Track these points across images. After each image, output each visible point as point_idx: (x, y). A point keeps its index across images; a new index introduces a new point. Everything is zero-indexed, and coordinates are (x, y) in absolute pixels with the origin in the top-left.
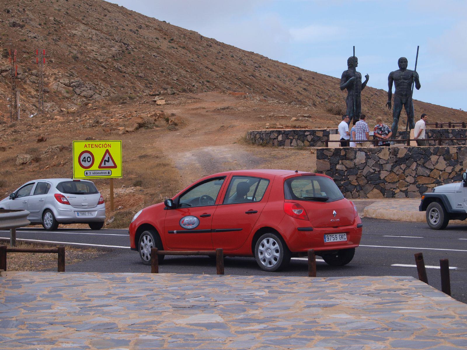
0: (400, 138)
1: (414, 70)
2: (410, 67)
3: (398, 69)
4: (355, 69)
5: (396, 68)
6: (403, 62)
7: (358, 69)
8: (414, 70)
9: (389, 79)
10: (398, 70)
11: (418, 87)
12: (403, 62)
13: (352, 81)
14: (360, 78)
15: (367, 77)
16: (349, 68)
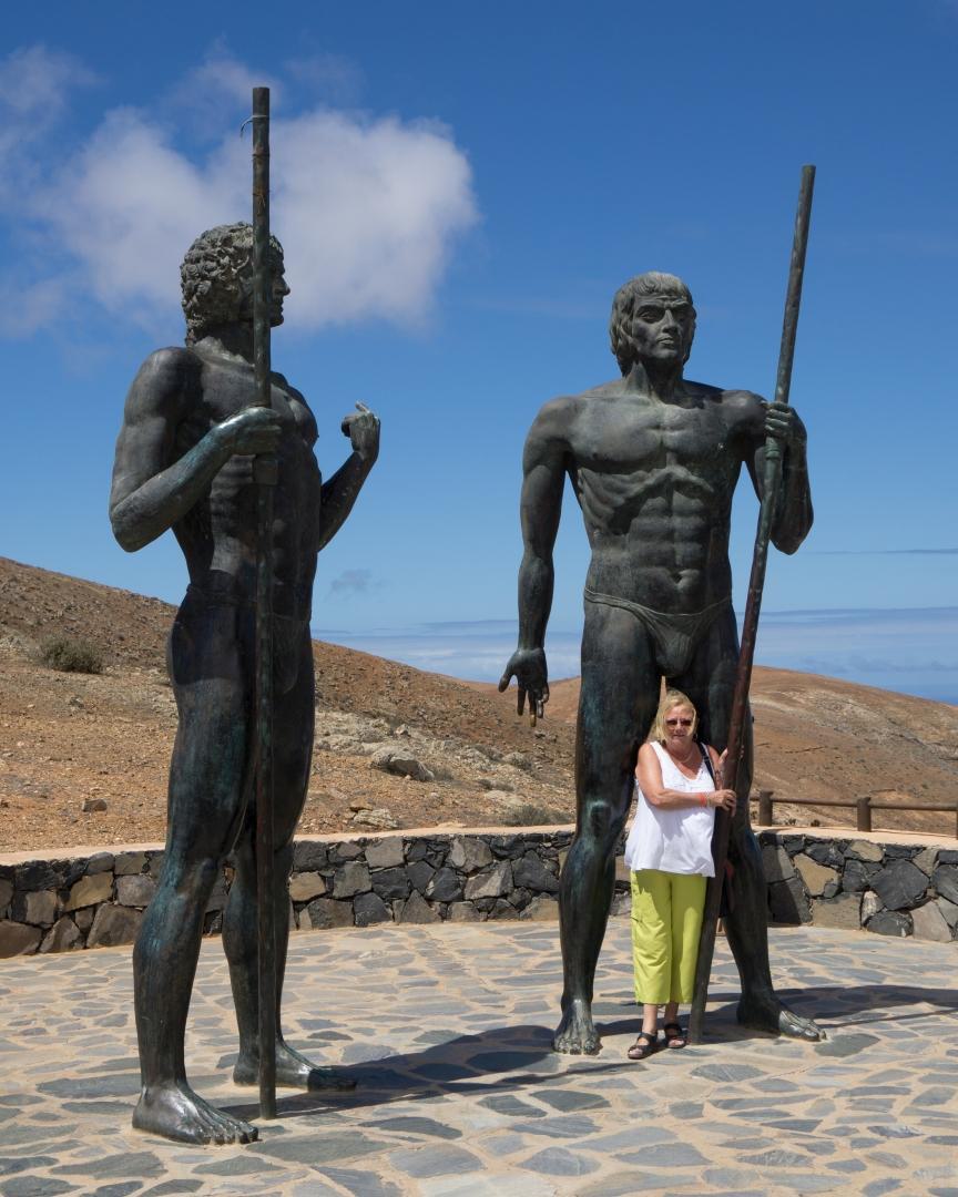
0: (492, 886)
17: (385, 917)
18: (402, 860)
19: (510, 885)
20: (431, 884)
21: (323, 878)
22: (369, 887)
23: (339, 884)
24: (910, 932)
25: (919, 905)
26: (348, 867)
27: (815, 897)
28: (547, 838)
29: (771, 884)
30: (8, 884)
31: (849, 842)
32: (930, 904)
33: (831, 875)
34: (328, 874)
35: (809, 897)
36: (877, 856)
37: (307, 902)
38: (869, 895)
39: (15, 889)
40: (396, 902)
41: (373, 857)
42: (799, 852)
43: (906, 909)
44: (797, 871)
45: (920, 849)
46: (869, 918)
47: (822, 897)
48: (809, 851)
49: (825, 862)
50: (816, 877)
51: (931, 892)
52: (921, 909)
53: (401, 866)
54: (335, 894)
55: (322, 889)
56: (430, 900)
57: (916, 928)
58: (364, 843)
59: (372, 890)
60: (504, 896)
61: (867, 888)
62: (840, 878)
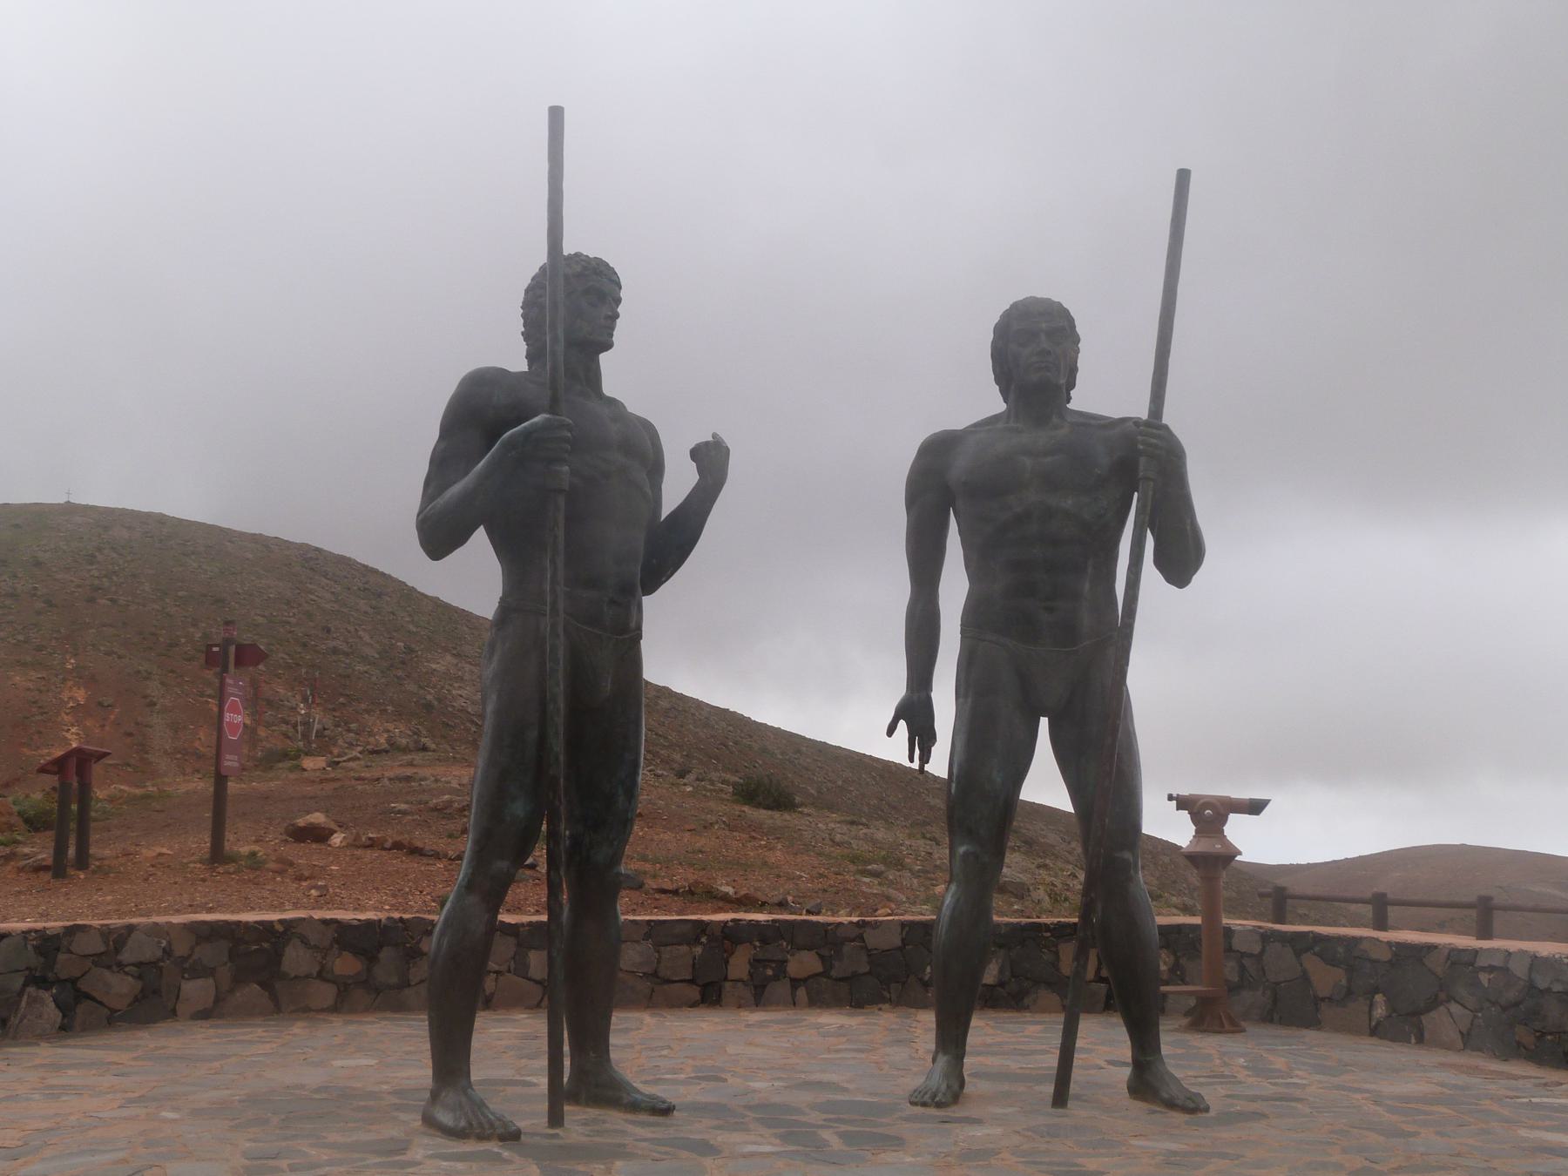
1: (1144, 414)
2: (1105, 388)
3: (995, 404)
4: (592, 378)
5: (976, 399)
6: (1034, 351)
7: (622, 375)
8: (1139, 409)
9: (912, 500)
10: (994, 419)
11: (1181, 559)
12: (1034, 351)
13: (557, 468)
14: (655, 468)
15: (711, 460)
16: (530, 357)
17: (883, 1000)
18: (898, 943)
19: (1008, 973)
20: (928, 969)
21: (822, 957)
22: (867, 969)
23: (837, 964)
24: (1420, 1040)
25: (1428, 1009)
26: (847, 948)
27: (1323, 999)
28: (1046, 927)
29: (1277, 984)
30: (512, 941)
31: (1356, 940)
32: (1442, 1008)
33: (1338, 976)
34: (825, 952)
35: (1318, 1001)
36: (1385, 956)
37: (805, 980)
38: (1379, 998)
39: (519, 945)
40: (893, 986)
41: (873, 940)
42: (1307, 950)
43: (1417, 1013)
44: (1305, 972)
45: (1431, 948)
46: (1378, 1023)
47: (1330, 999)
48: (1317, 949)
49: (1332, 962)
50: (1326, 978)
51: (1442, 996)
52: (1433, 1014)
53: (900, 949)
54: (833, 973)
55: (820, 969)
56: (926, 985)
57: (1427, 1035)
58: (861, 925)
59: (870, 973)
60: (1001, 984)
61: (1376, 990)
62: (1349, 981)
